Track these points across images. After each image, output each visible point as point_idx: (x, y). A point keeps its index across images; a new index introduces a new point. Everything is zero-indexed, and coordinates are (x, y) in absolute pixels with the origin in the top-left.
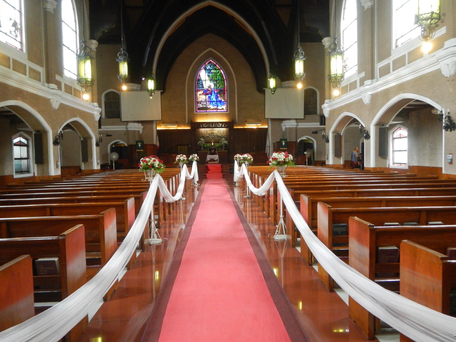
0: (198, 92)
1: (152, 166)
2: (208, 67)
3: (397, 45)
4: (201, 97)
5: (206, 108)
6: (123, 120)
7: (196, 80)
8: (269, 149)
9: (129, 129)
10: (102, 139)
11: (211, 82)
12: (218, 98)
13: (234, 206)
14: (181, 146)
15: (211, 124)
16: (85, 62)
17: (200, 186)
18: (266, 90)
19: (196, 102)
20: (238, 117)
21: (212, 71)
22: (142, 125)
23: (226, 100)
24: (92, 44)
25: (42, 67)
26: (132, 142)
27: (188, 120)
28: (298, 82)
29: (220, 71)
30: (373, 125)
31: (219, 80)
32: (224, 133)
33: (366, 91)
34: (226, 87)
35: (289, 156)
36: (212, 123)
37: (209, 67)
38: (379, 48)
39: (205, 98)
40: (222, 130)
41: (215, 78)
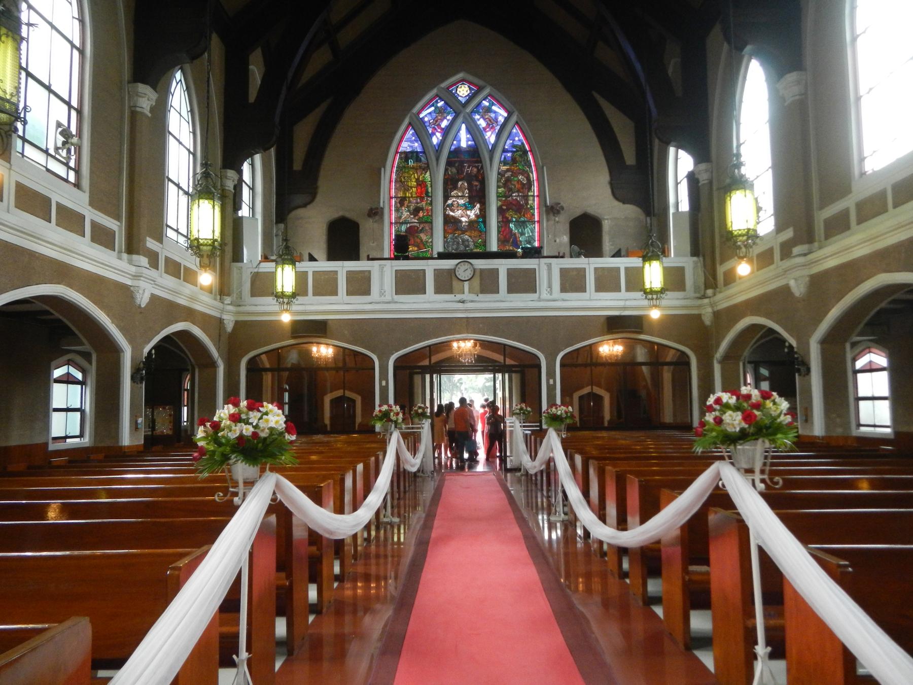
3: (863, 172)
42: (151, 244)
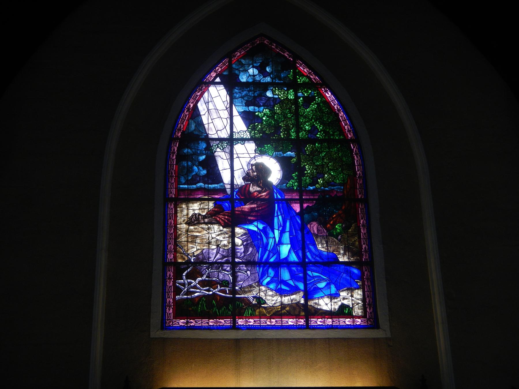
21: (269, 94)
29: (322, 96)
31: (313, 141)
34: (360, 181)
41: (287, 130)
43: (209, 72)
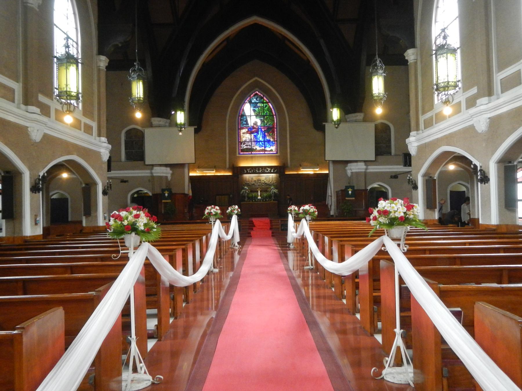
0: (242, 130)
1: (133, 228)
2: (254, 100)
4: (246, 137)
5: (251, 150)
6: (147, 163)
7: (239, 116)
8: (331, 199)
9: (154, 175)
10: (110, 185)
11: (257, 118)
12: (266, 137)
13: (292, 286)
14: (220, 196)
15: (257, 169)
16: (67, 68)
17: (241, 248)
18: (326, 125)
19: (239, 142)
20: (291, 160)
21: (258, 105)
22: (171, 170)
23: (276, 140)
24: (100, 60)
25: (17, 82)
26: (158, 191)
27: (229, 165)
28: (376, 105)
29: (269, 105)
30: (494, 162)
31: (266, 115)
32: (274, 180)
33: (481, 113)
34: (275, 124)
35: (414, 206)
36: (259, 168)
37: (255, 100)
38: (498, 51)
39: (250, 137)
40: (271, 177)
41: (262, 113)
42: (42, 98)
43: (246, 100)
